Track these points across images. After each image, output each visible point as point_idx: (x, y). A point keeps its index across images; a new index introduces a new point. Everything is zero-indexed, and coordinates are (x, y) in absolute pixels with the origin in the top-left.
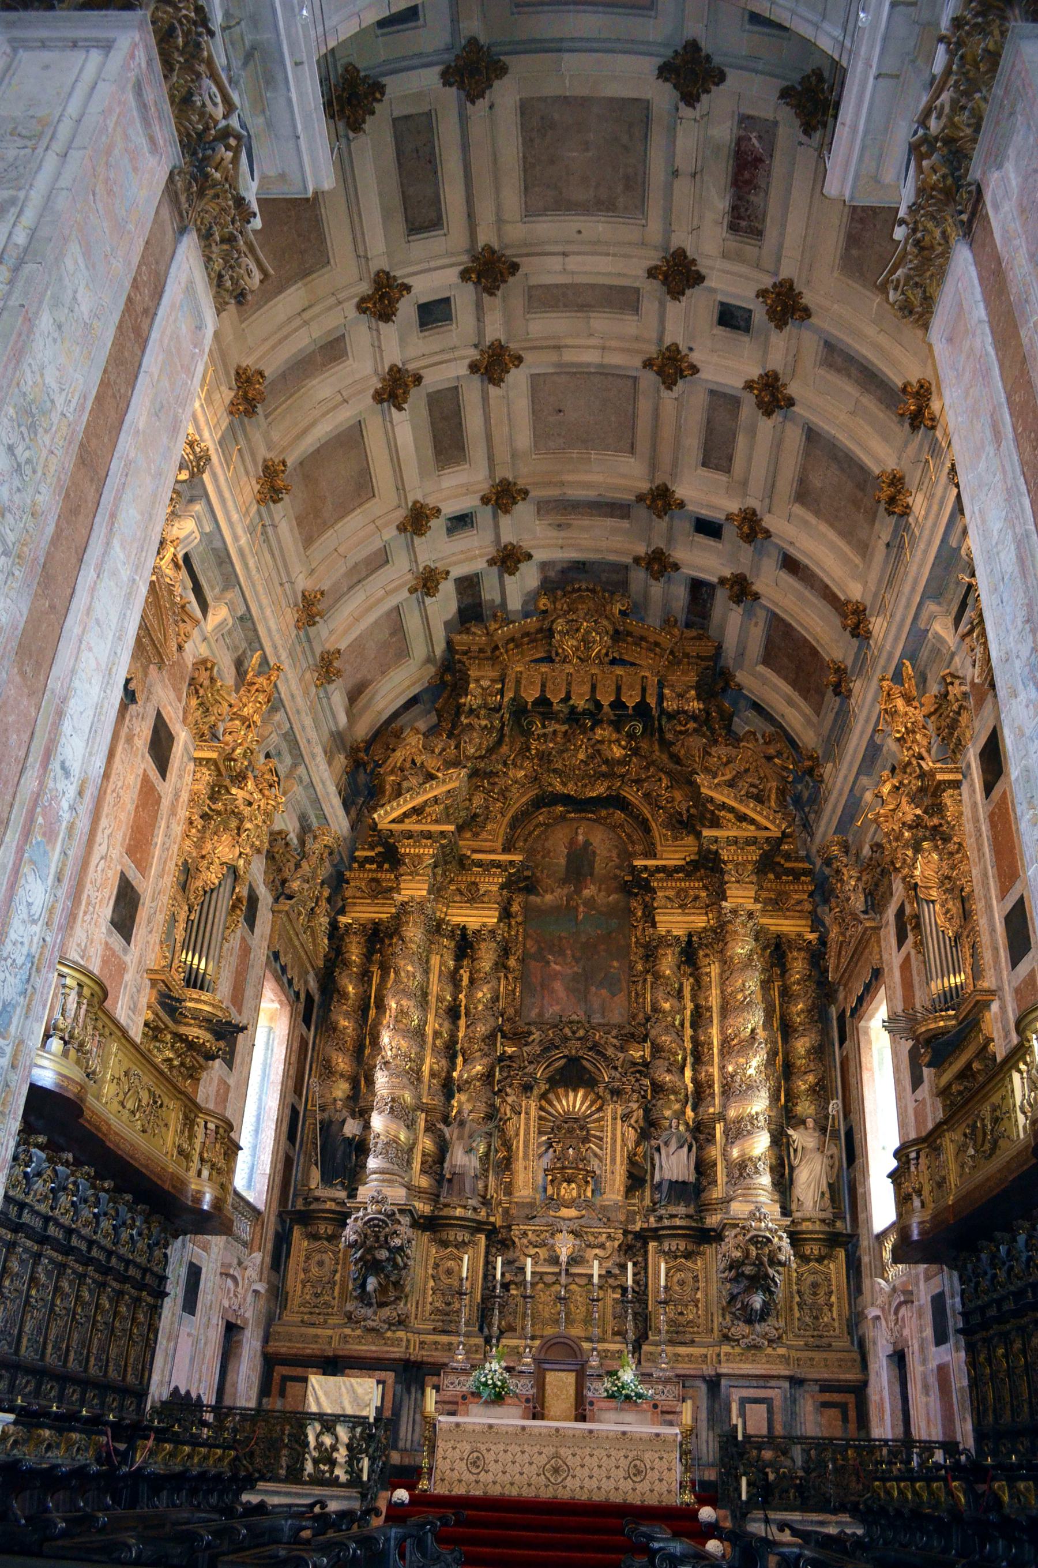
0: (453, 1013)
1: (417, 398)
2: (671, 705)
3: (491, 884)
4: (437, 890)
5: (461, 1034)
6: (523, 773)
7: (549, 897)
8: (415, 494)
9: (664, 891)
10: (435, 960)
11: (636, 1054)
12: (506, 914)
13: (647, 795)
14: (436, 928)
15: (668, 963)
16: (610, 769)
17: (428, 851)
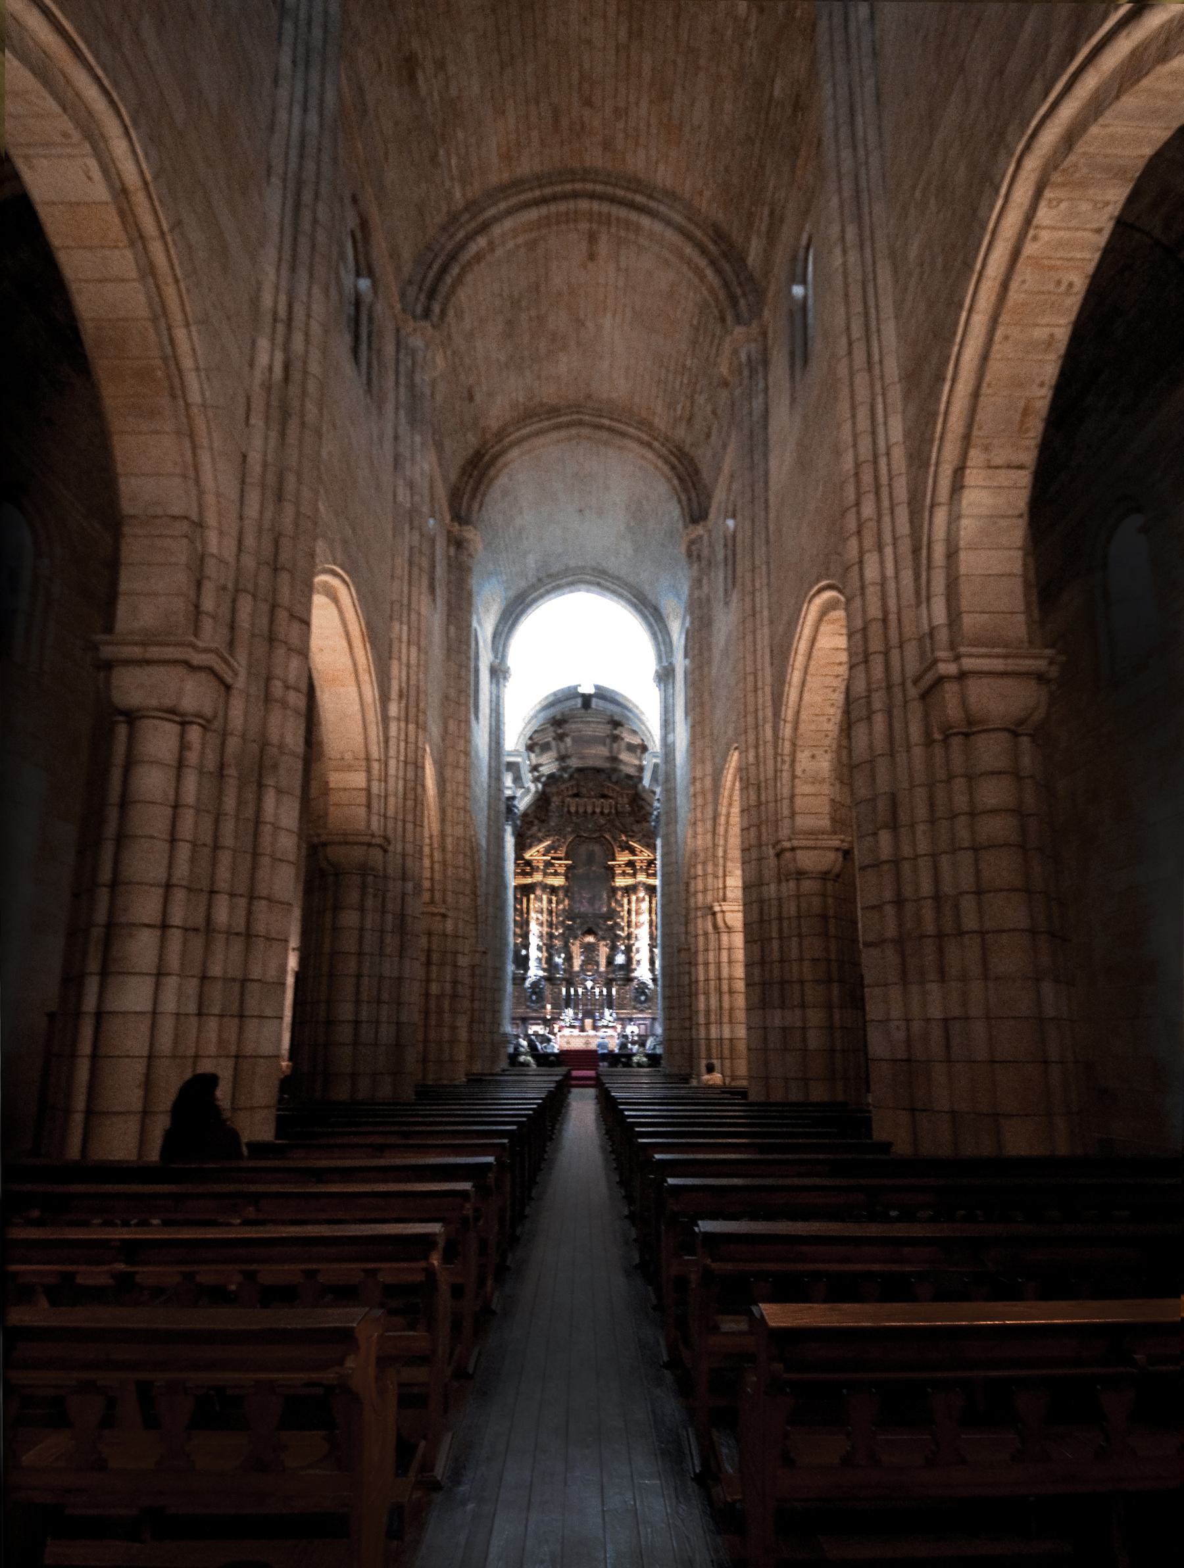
0: (550, 912)
1: (537, 749)
2: (620, 809)
3: (562, 870)
4: (545, 874)
5: (554, 919)
6: (569, 829)
7: (581, 871)
8: (534, 762)
9: (618, 871)
10: (545, 897)
11: (610, 923)
12: (567, 878)
13: (613, 837)
14: (545, 887)
15: (620, 893)
16: (601, 828)
17: (541, 866)
